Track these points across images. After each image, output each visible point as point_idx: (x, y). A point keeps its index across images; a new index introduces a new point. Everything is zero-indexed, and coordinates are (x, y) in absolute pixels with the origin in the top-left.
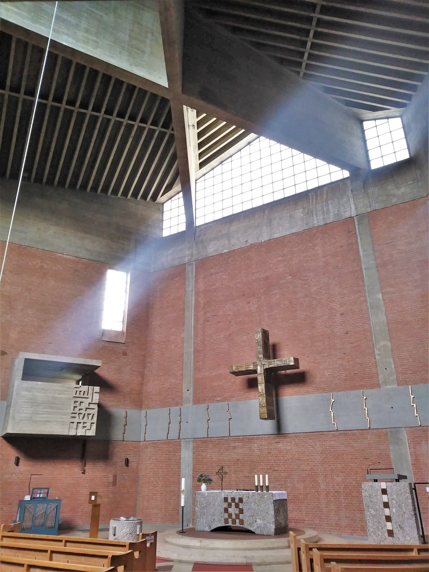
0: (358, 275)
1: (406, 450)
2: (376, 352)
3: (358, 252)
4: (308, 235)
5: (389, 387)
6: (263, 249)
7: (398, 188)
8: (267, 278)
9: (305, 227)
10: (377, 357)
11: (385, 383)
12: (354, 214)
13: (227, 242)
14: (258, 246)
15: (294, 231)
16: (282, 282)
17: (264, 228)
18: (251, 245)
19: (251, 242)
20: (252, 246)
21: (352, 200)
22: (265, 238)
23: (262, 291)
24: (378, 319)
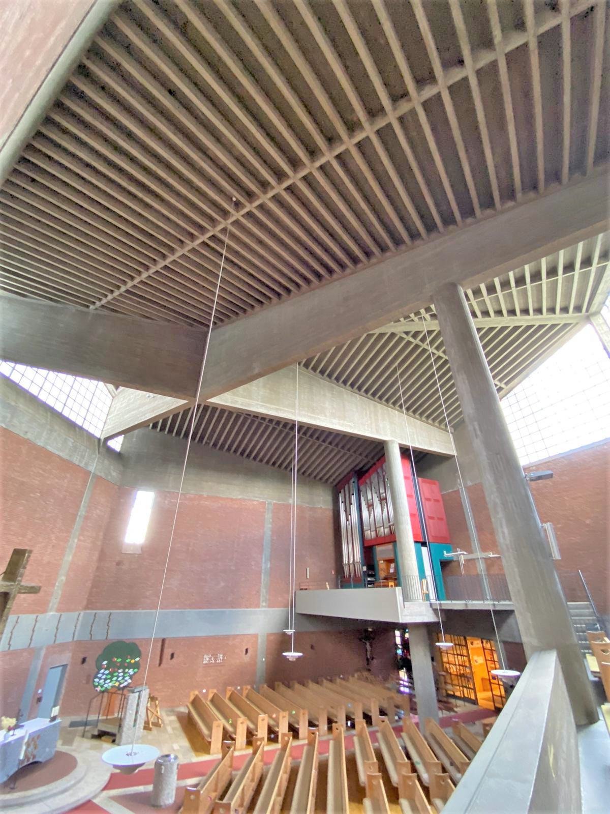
0: (75, 516)
1: (40, 662)
2: (57, 584)
3: (81, 501)
4: (66, 465)
5: (52, 613)
6: (34, 452)
7: (114, 471)
8: (23, 483)
9: (68, 458)
10: (56, 588)
11: (51, 610)
12: (92, 472)
13: (9, 415)
14: (32, 446)
15: (61, 454)
16: (32, 495)
17: (45, 433)
18: (28, 439)
19: (29, 436)
20: (27, 442)
21: (96, 459)
22: (41, 443)
23: (13, 494)
24: (68, 558)
